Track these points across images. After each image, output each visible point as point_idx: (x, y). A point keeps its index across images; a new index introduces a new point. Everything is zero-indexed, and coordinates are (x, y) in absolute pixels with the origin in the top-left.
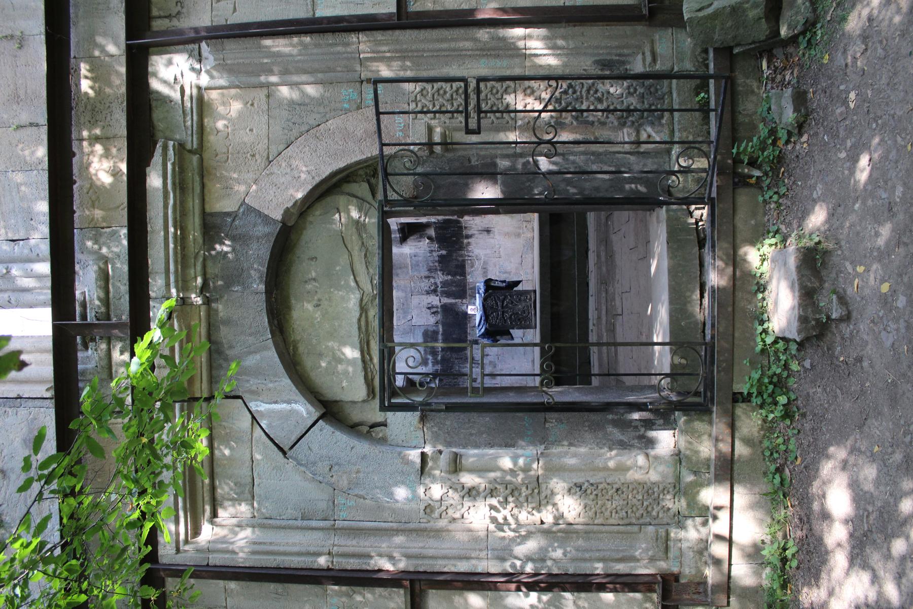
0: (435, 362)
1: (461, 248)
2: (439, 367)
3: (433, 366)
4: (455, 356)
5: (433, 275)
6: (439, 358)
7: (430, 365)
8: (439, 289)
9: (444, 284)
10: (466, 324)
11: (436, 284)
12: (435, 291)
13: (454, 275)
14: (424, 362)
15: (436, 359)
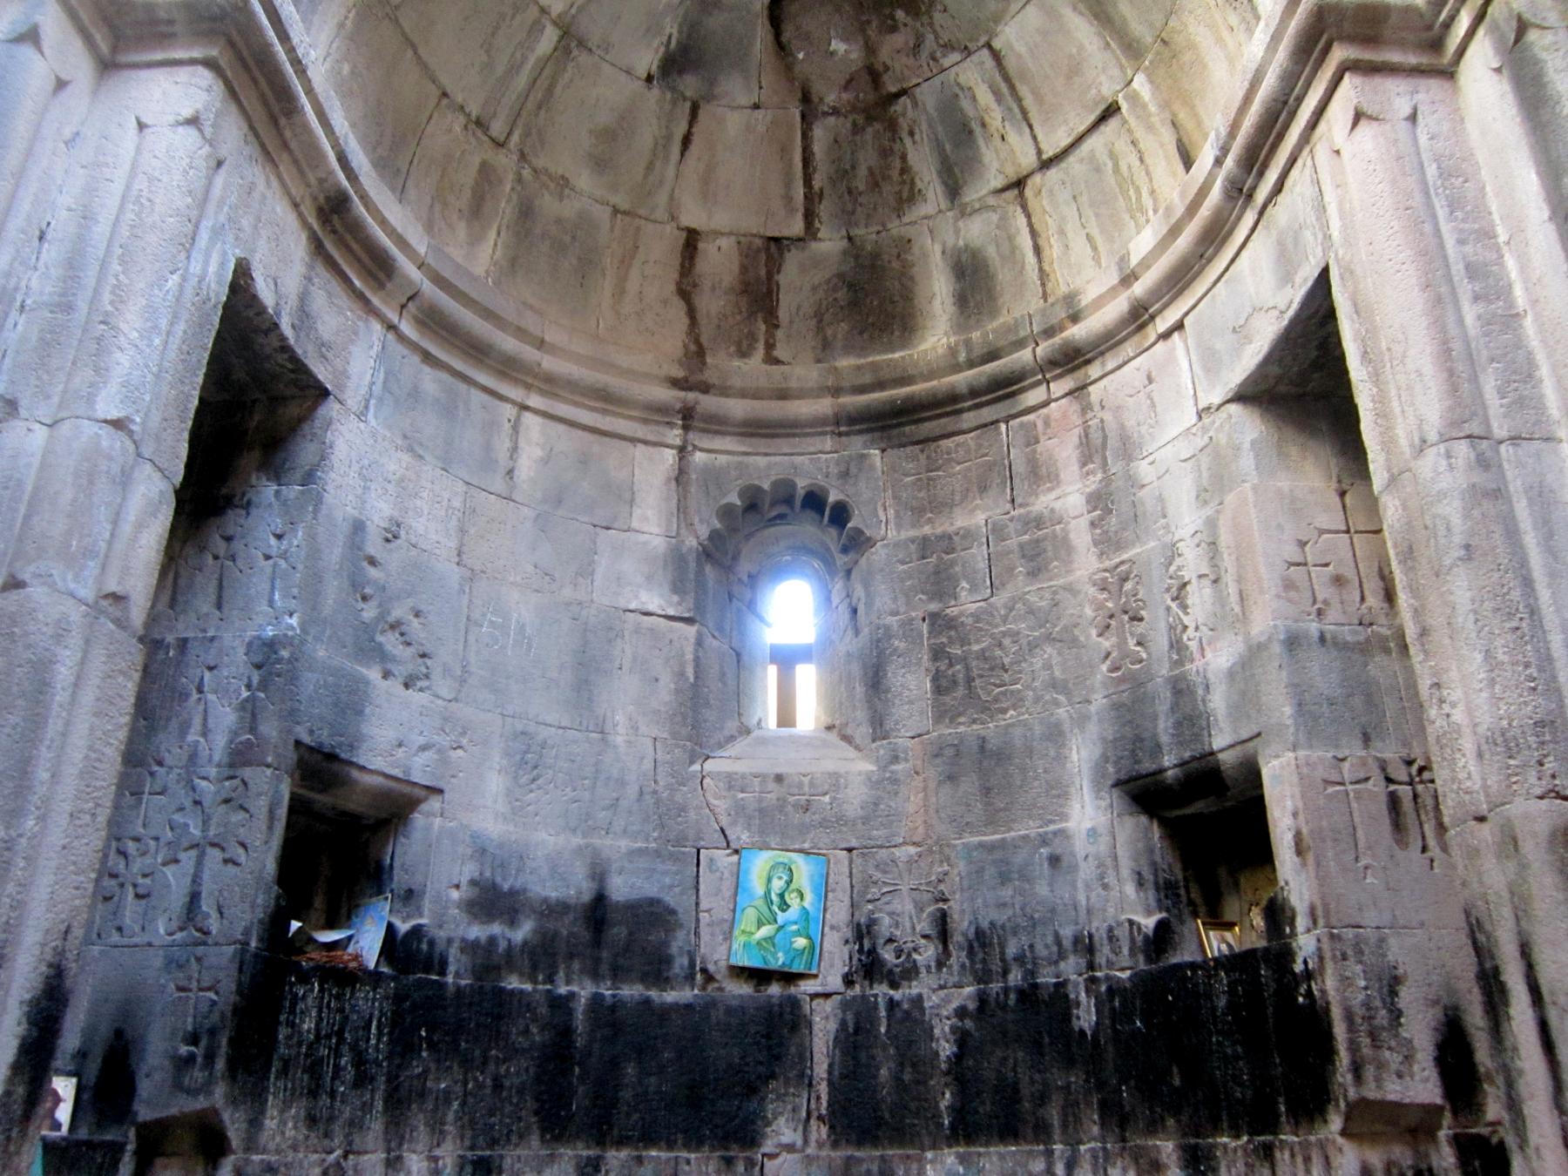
0: (488, 961)
1: (1117, 1119)
2: (457, 975)
3: (470, 947)
4: (518, 1072)
5: (958, 957)
6: (513, 983)
7: (477, 932)
8: (882, 990)
9: (910, 1019)
10: (694, 1140)
11: (911, 972)
12: (869, 967)
13: (959, 1071)
14: (491, 900)
15: (509, 961)
